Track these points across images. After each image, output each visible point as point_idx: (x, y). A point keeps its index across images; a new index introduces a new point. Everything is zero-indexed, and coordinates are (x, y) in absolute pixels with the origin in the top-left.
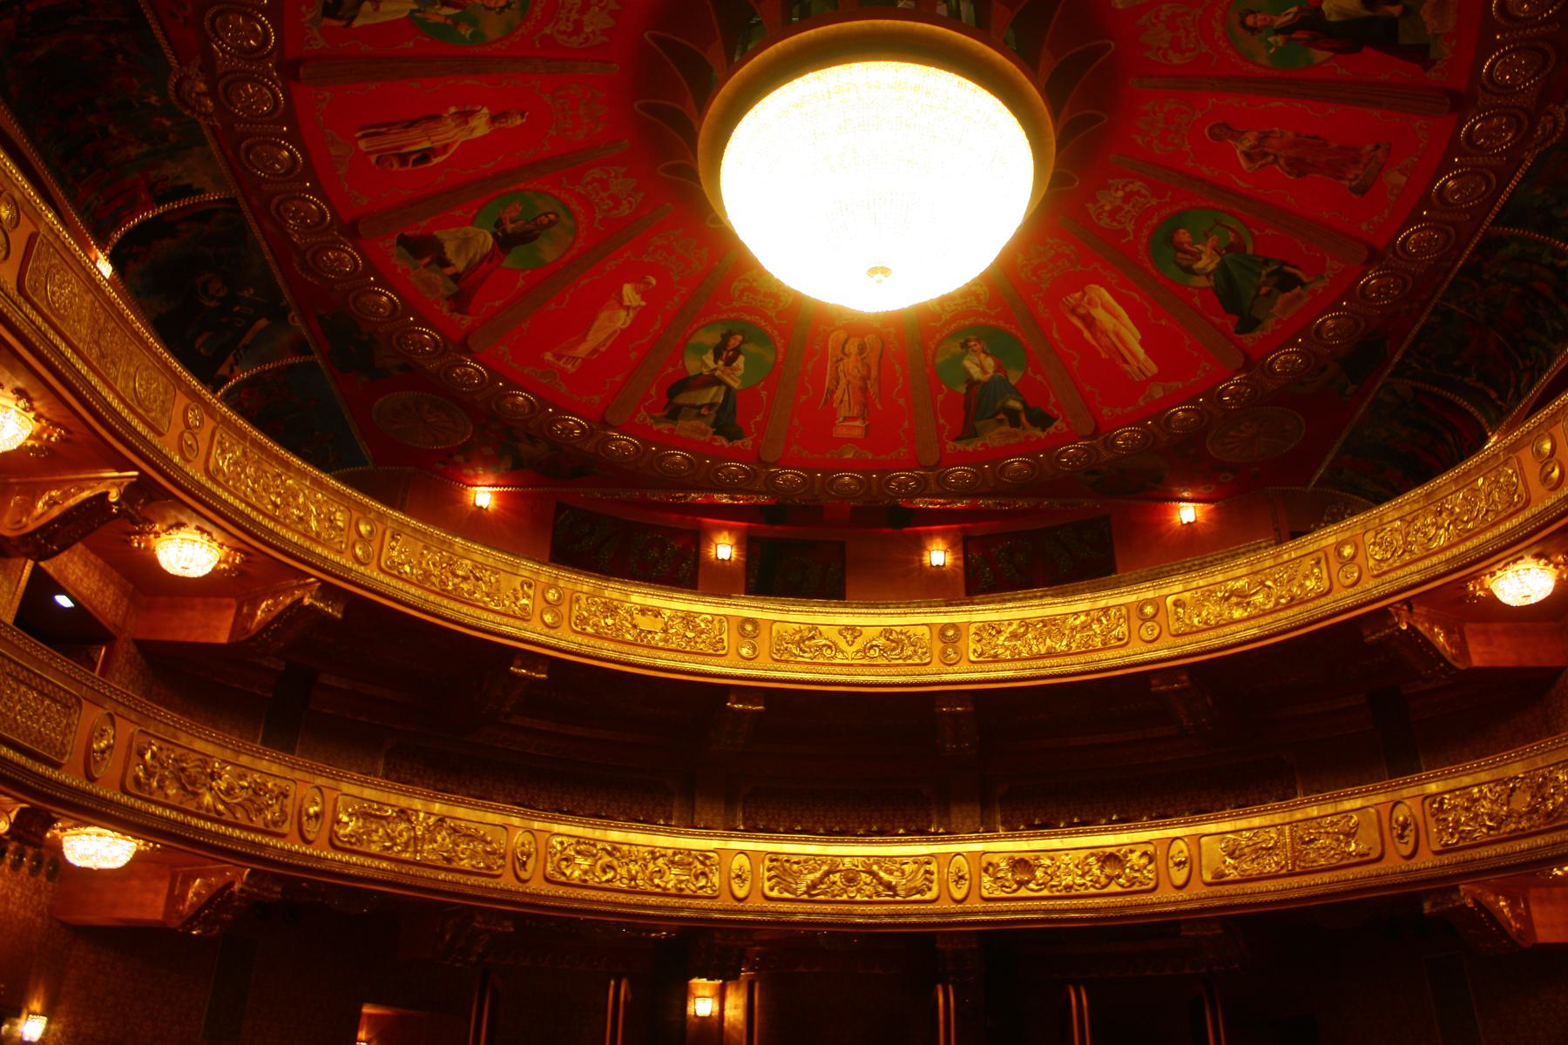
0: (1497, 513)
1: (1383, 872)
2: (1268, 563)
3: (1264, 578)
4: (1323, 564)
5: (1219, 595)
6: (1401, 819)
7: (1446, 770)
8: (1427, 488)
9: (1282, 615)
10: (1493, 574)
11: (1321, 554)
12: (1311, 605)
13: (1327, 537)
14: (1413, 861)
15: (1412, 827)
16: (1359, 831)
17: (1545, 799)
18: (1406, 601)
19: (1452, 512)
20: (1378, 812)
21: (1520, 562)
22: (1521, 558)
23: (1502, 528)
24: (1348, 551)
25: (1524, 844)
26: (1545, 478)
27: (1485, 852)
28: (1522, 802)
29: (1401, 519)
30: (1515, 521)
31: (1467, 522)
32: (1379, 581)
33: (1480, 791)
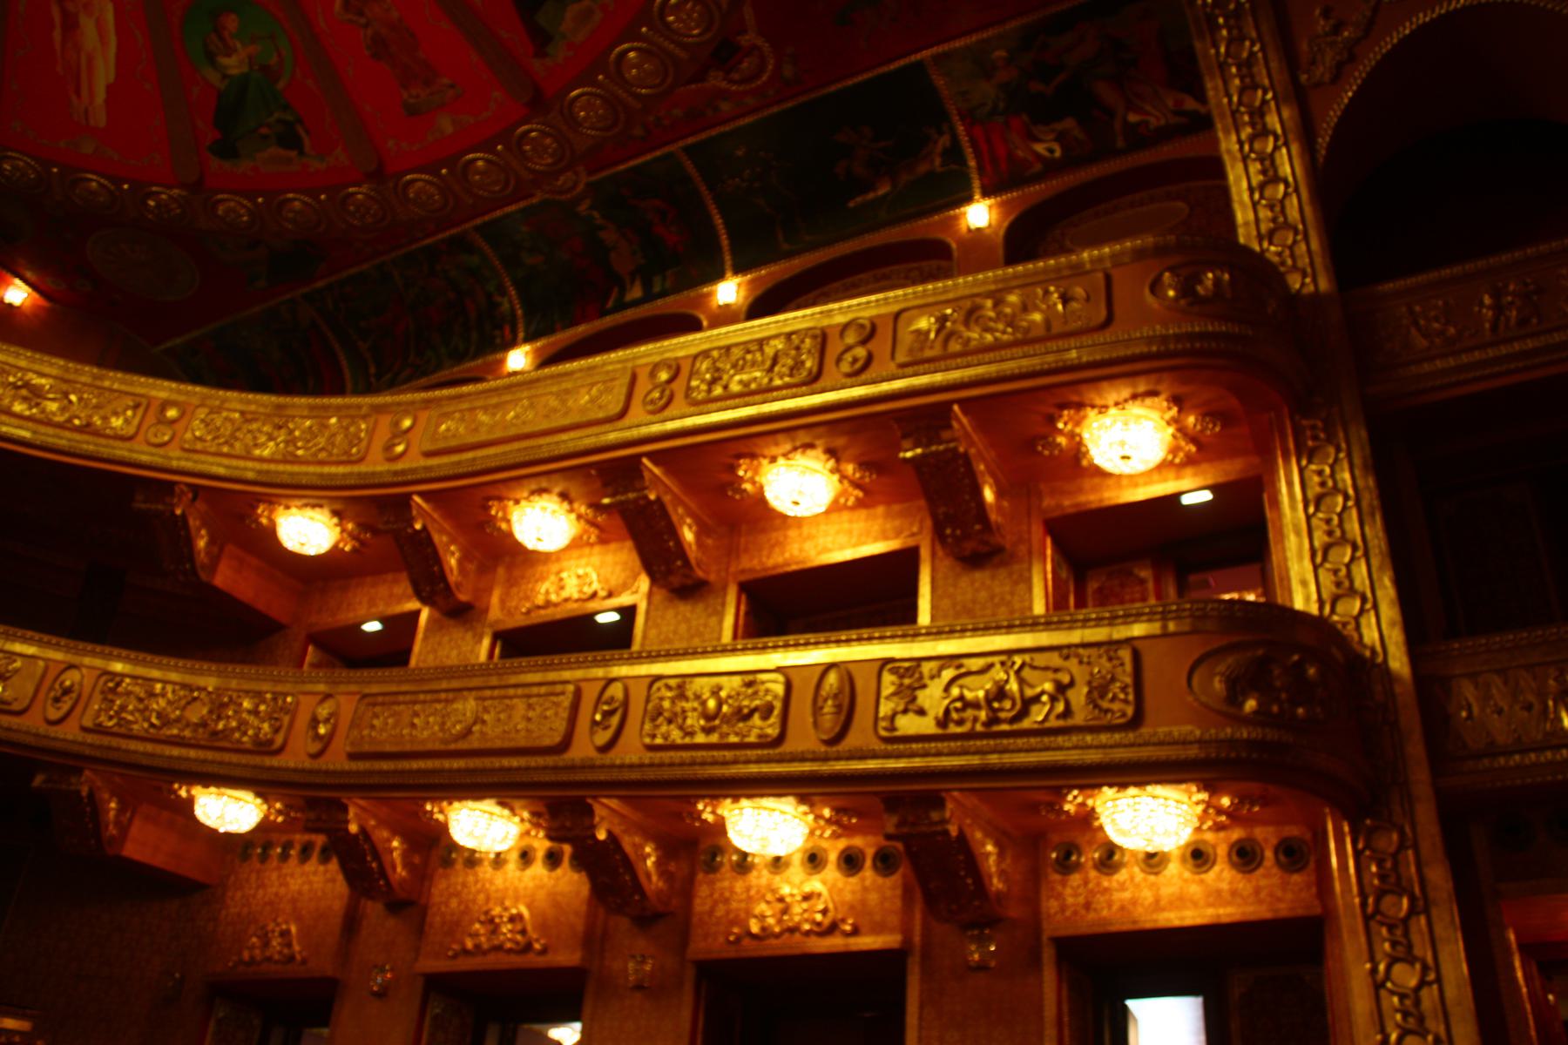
0: (331, 454)
1: (15, 727)
2: (84, 379)
3: (70, 390)
4: (140, 412)
5: (11, 379)
6: (68, 683)
7: (141, 656)
8: (282, 400)
9: (68, 434)
10: (287, 507)
11: (144, 401)
12: (103, 441)
13: (162, 389)
14: (54, 729)
15: (74, 695)
16: (15, 679)
17: (219, 718)
18: (195, 489)
19: (291, 432)
20: (46, 668)
21: (318, 510)
22: (321, 506)
23: (326, 469)
24: (172, 413)
25: (176, 752)
26: (389, 447)
27: (133, 745)
28: (197, 713)
29: (242, 413)
30: (341, 469)
31: (299, 448)
32: (186, 455)
33: (163, 688)
